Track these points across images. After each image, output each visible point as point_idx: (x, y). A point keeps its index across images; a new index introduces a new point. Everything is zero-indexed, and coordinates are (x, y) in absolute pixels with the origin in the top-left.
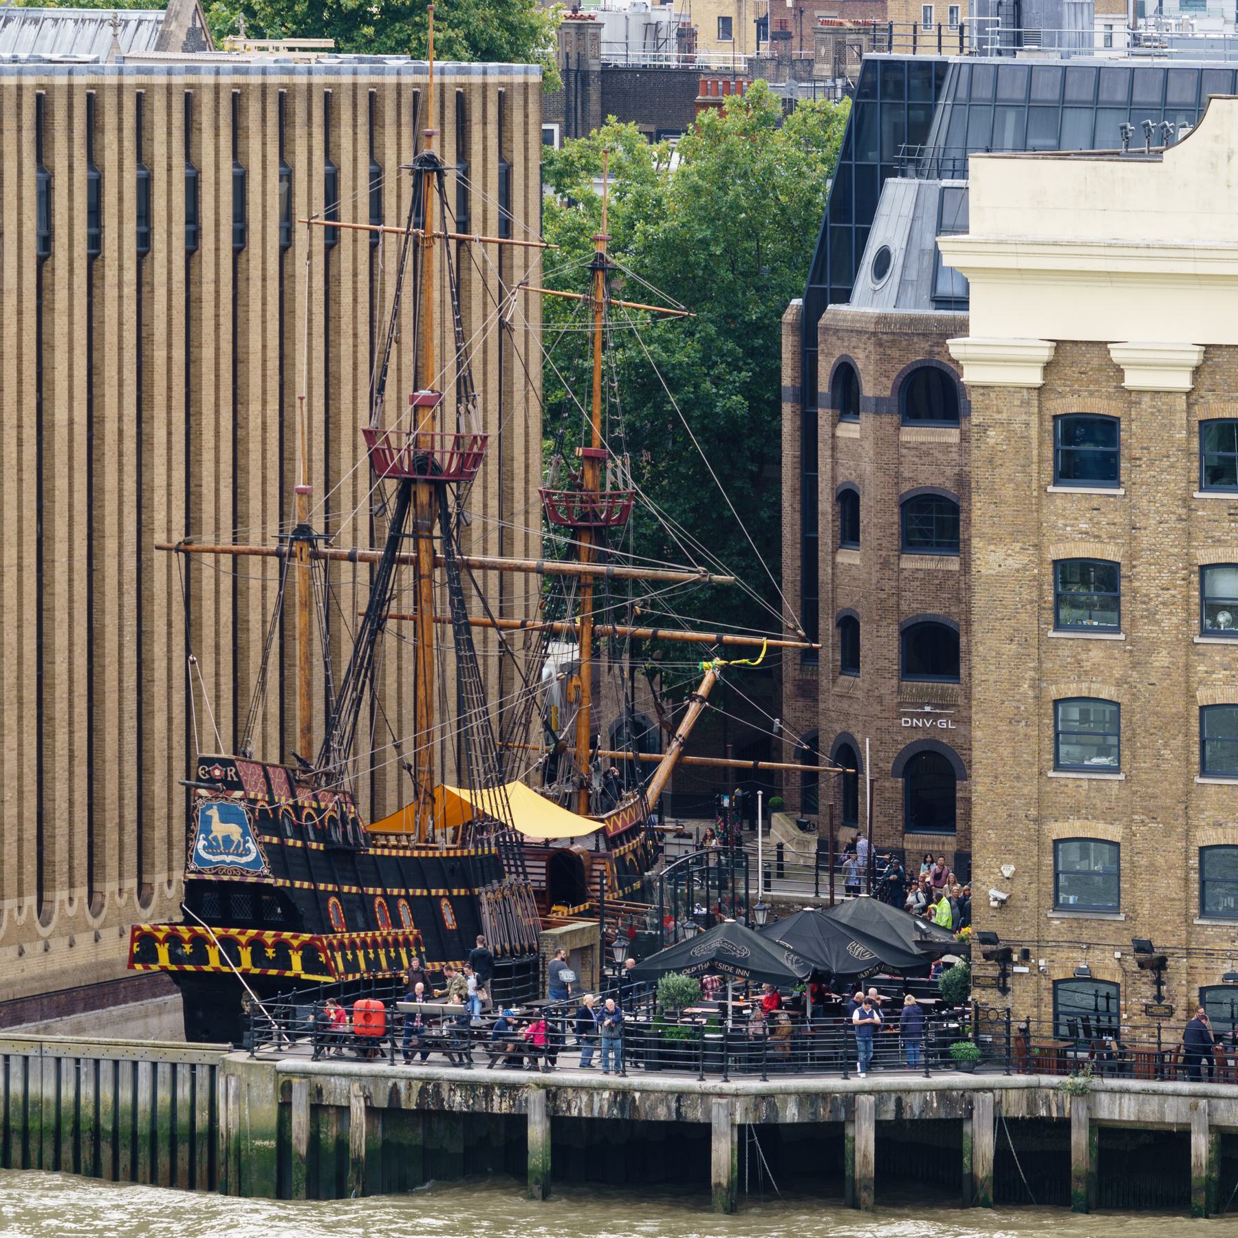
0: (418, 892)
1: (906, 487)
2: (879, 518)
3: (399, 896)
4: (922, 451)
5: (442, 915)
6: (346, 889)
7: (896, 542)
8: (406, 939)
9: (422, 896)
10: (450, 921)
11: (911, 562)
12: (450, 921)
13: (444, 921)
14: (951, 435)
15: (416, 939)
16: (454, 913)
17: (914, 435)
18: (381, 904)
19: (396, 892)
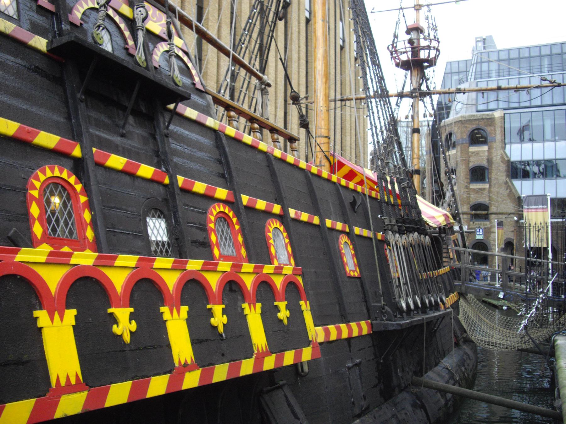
0: (305, 217)
1: (471, 165)
2: (462, 174)
3: (268, 214)
4: (477, 154)
5: (341, 256)
6: (117, 161)
7: (469, 180)
8: (265, 287)
9: (309, 224)
10: (351, 265)
11: (473, 186)
12: (351, 265)
13: (344, 265)
14: (485, 148)
15: (291, 285)
16: (356, 255)
17: (473, 149)
18: (223, 217)
19: (261, 205)
